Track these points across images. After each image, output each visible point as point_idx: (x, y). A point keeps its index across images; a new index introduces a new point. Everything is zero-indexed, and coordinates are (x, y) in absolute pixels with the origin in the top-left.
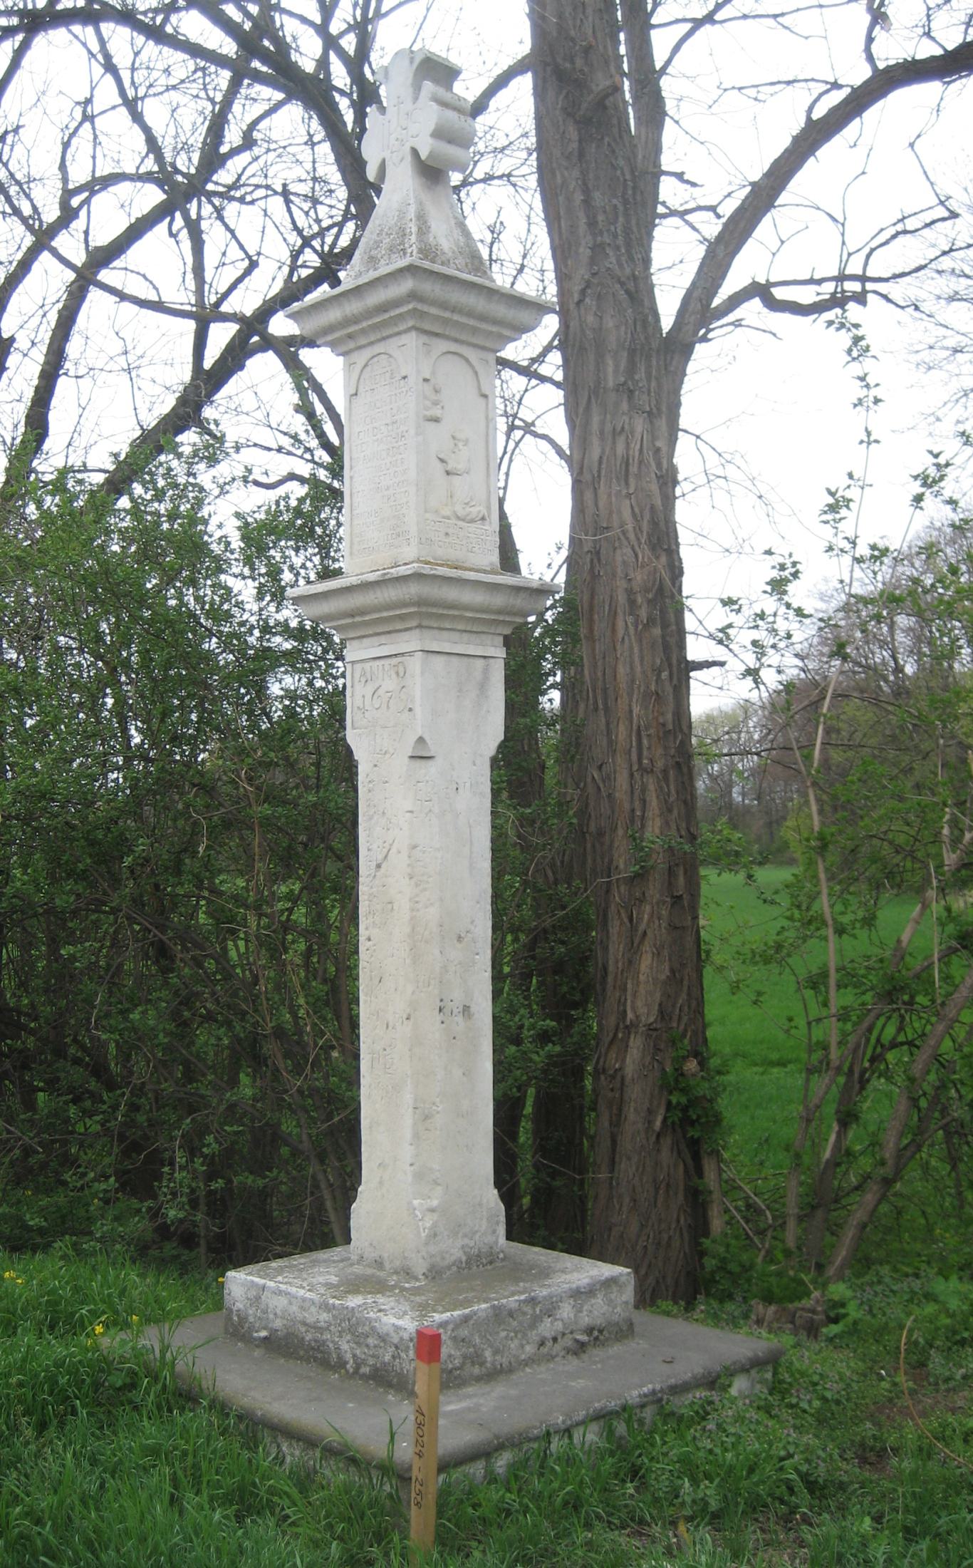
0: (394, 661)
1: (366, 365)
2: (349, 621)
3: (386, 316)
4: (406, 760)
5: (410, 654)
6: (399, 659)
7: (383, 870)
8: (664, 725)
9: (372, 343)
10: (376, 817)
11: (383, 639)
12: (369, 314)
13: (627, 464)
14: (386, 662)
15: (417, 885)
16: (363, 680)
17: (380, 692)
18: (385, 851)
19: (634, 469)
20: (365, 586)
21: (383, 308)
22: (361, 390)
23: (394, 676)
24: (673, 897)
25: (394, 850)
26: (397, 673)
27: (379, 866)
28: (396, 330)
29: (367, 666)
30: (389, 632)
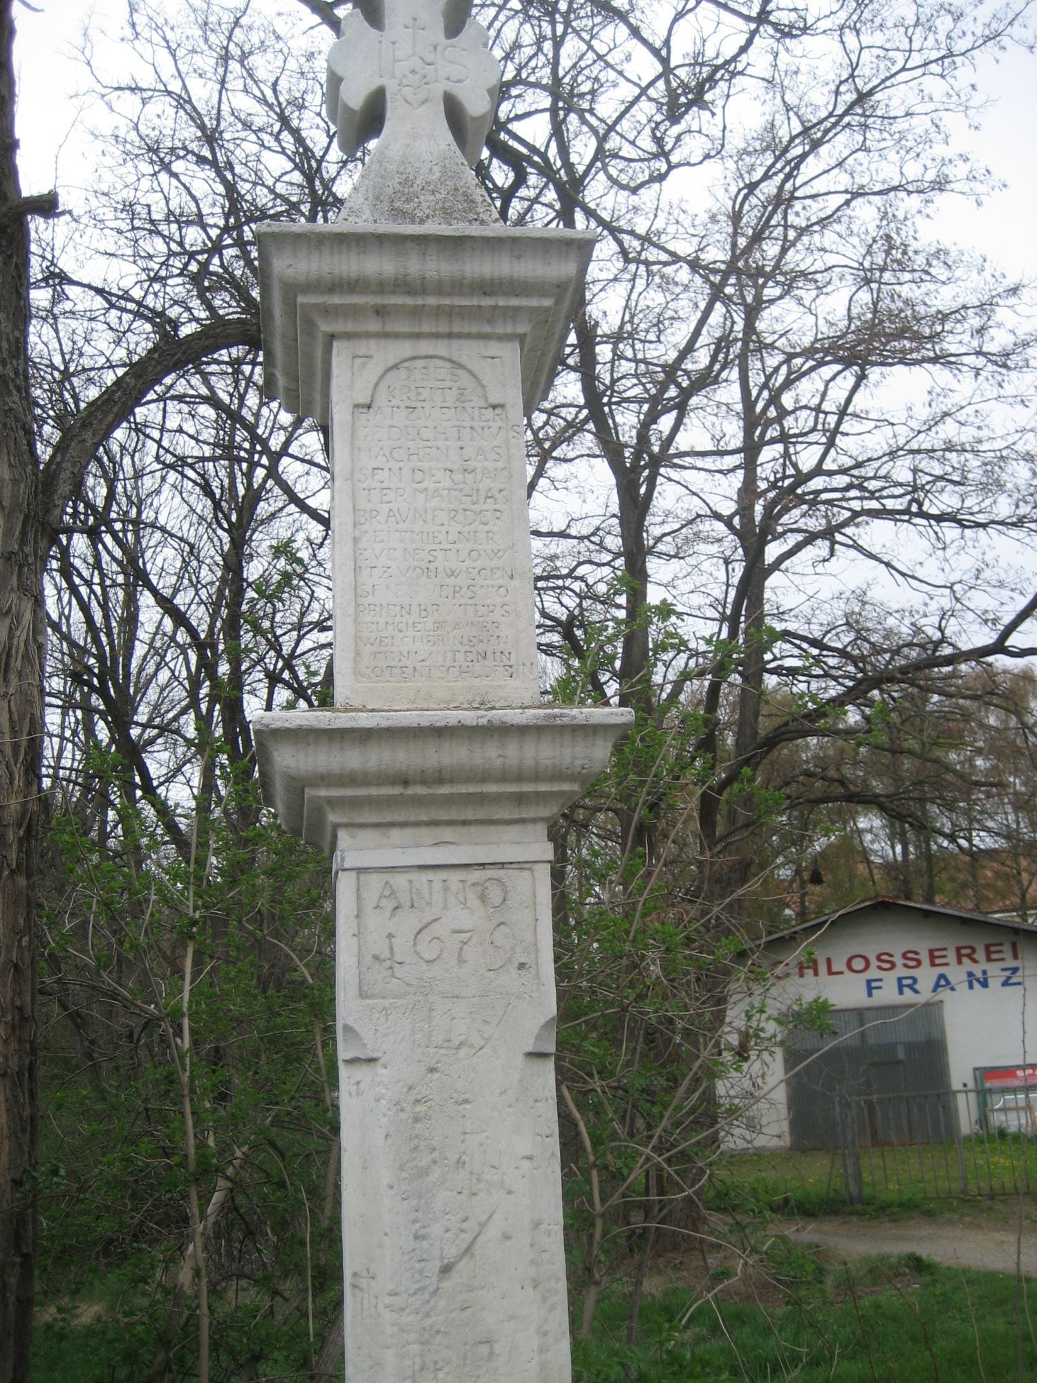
0: (476, 875)
1: (395, 367)
2: (397, 790)
3: (487, 302)
4: (520, 1060)
5: (521, 865)
6: (490, 873)
7: (455, 1278)
8: (20, 1009)
9: (418, 336)
10: (437, 1172)
11: (447, 833)
12: (458, 286)
13: (9, 656)
14: (454, 877)
15: (544, 1299)
16: (388, 905)
17: (440, 929)
18: (468, 1237)
19: (17, 664)
20: (365, 736)
21: (486, 287)
22: (381, 399)
23: (473, 901)
24: (22, 1256)
25: (492, 1233)
26: (483, 898)
27: (446, 1270)
28: (487, 329)
29: (400, 880)
30: (465, 823)
